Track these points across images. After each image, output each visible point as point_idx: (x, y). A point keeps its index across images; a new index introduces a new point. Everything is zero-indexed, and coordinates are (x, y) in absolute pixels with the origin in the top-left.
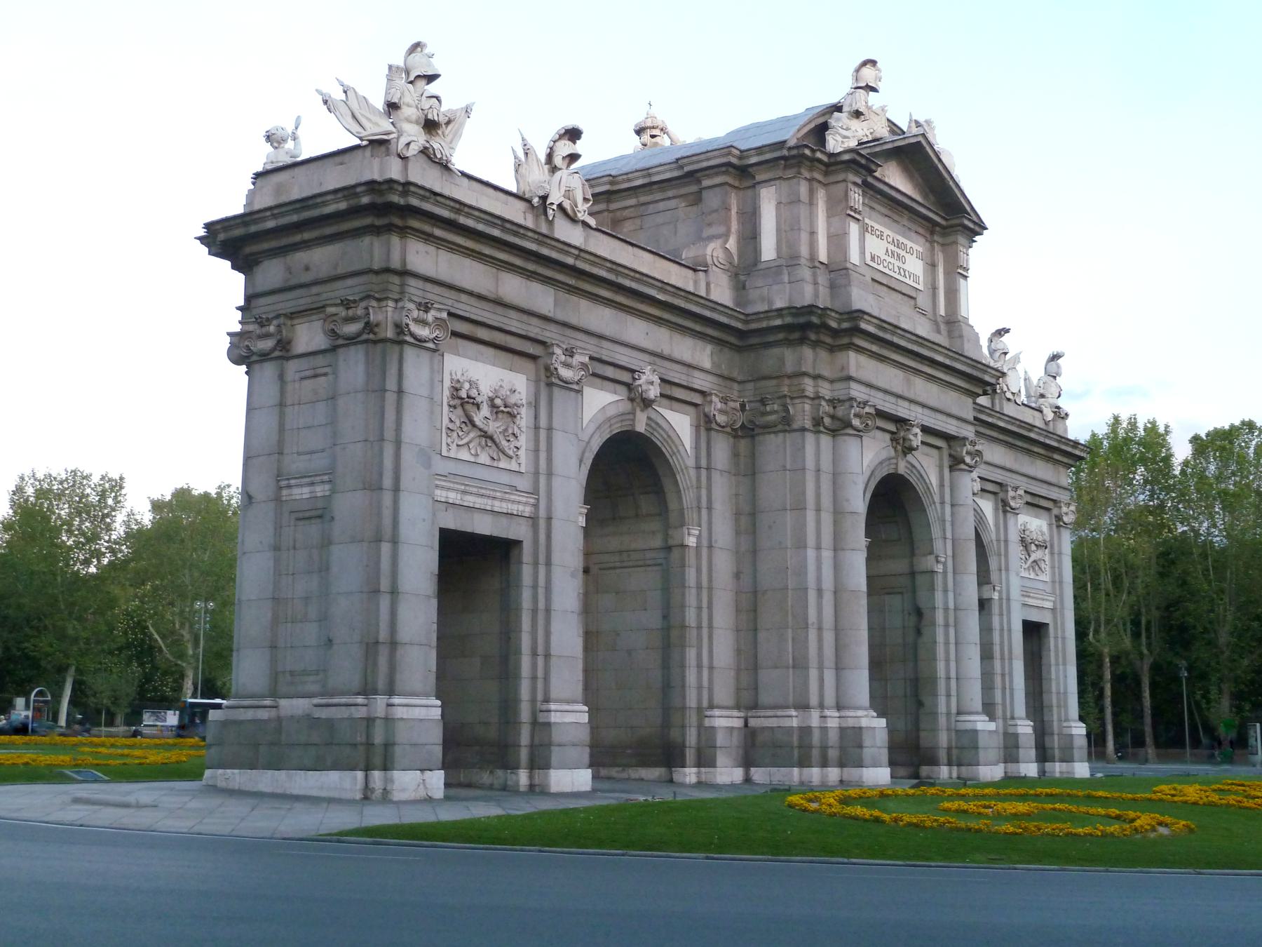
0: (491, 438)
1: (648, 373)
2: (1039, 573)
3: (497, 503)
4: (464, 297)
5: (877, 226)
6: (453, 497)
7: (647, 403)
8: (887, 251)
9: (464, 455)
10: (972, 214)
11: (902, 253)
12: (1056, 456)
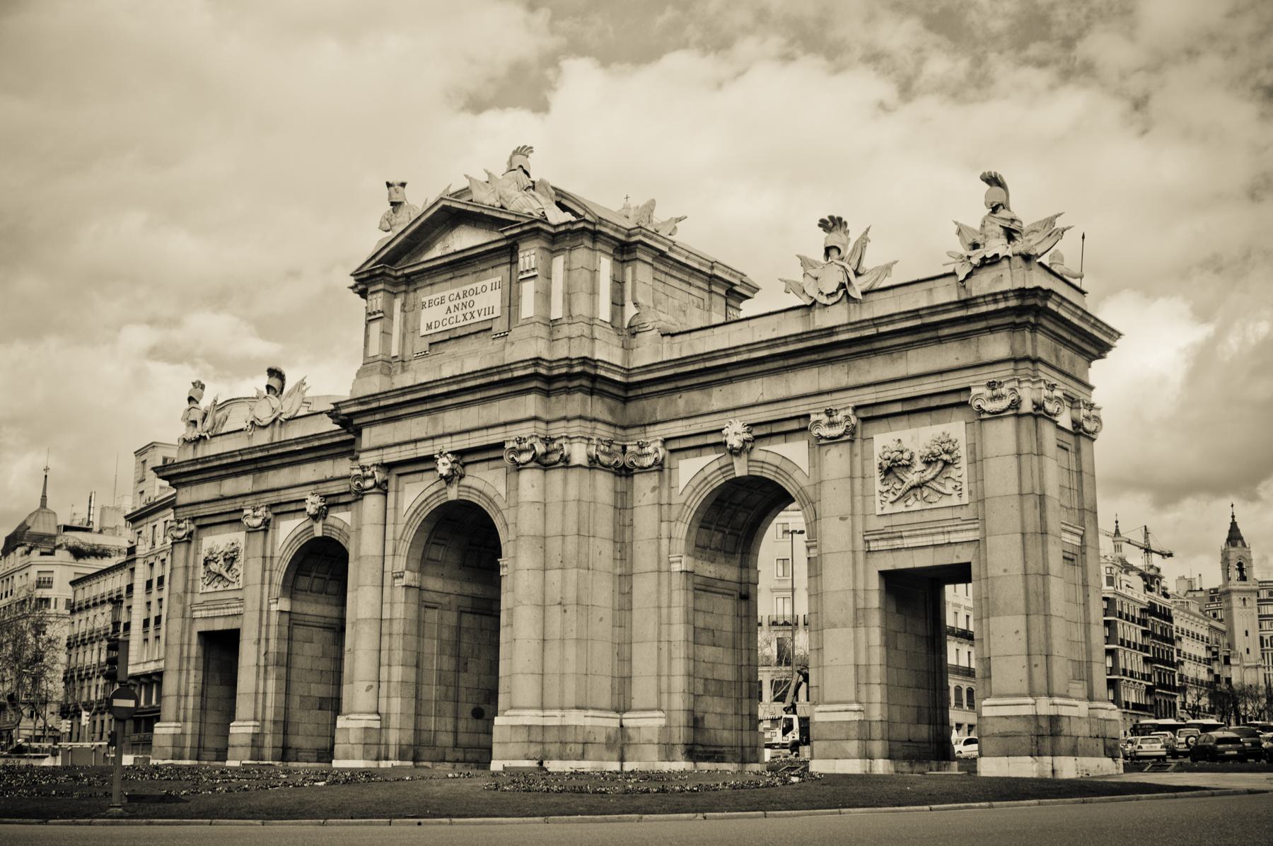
0: (220, 575)
1: (309, 497)
2: (934, 497)
3: (226, 610)
4: (202, 506)
5: (433, 297)
6: (204, 613)
7: (315, 517)
8: (449, 309)
9: (210, 589)
10: (521, 219)
11: (468, 299)
12: (946, 331)
